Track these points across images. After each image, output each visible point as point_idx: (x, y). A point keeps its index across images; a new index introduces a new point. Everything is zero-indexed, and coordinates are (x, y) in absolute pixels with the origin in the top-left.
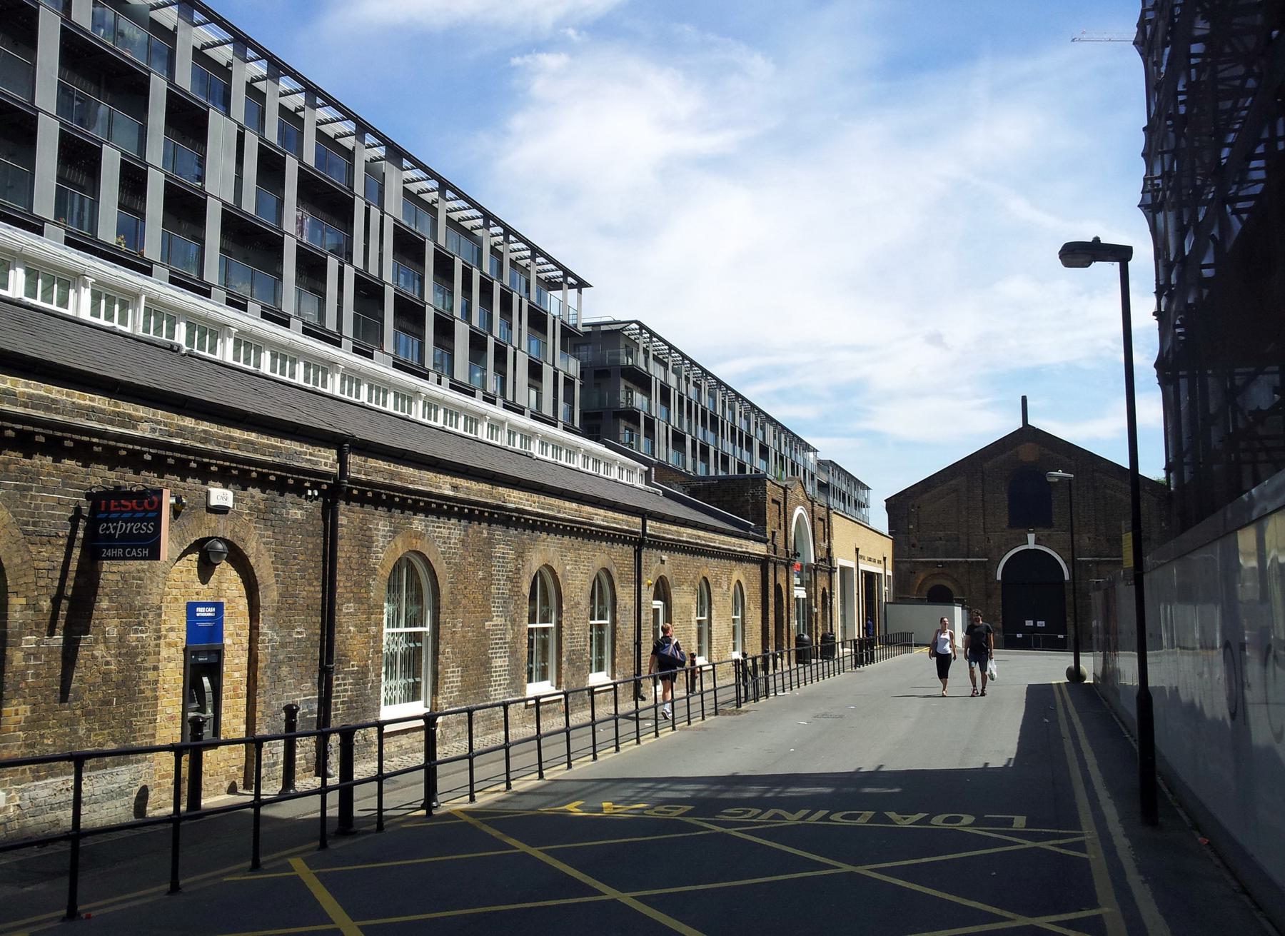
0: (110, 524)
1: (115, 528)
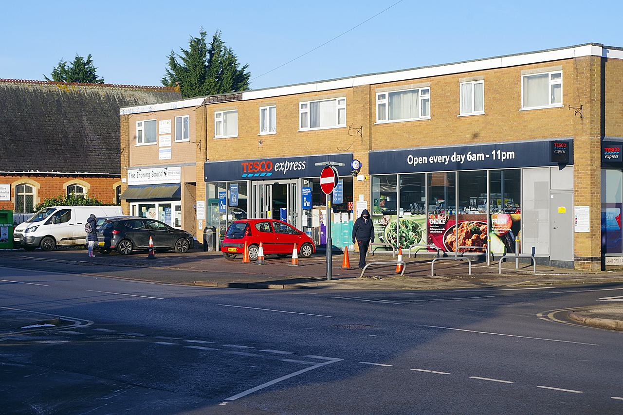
0: (281, 164)
1: (284, 166)
